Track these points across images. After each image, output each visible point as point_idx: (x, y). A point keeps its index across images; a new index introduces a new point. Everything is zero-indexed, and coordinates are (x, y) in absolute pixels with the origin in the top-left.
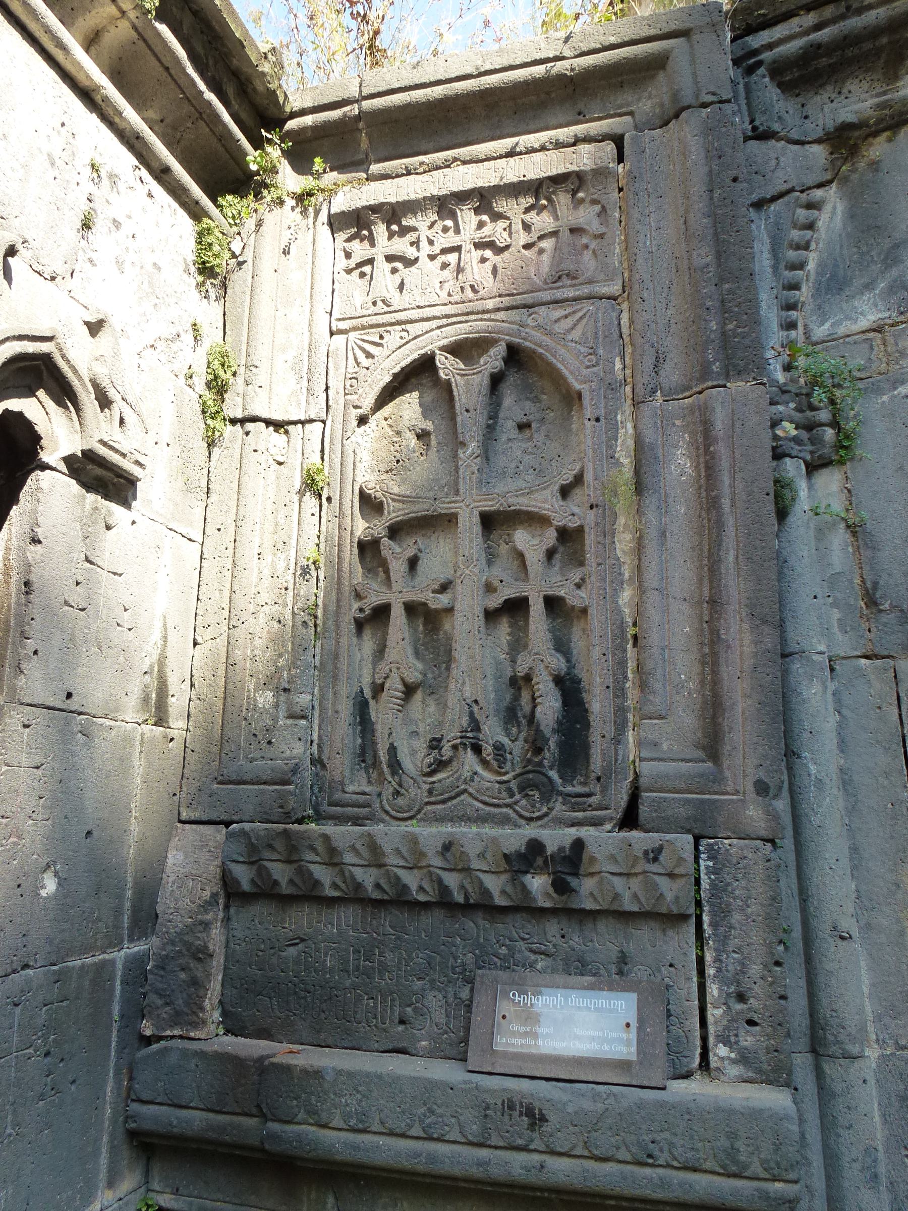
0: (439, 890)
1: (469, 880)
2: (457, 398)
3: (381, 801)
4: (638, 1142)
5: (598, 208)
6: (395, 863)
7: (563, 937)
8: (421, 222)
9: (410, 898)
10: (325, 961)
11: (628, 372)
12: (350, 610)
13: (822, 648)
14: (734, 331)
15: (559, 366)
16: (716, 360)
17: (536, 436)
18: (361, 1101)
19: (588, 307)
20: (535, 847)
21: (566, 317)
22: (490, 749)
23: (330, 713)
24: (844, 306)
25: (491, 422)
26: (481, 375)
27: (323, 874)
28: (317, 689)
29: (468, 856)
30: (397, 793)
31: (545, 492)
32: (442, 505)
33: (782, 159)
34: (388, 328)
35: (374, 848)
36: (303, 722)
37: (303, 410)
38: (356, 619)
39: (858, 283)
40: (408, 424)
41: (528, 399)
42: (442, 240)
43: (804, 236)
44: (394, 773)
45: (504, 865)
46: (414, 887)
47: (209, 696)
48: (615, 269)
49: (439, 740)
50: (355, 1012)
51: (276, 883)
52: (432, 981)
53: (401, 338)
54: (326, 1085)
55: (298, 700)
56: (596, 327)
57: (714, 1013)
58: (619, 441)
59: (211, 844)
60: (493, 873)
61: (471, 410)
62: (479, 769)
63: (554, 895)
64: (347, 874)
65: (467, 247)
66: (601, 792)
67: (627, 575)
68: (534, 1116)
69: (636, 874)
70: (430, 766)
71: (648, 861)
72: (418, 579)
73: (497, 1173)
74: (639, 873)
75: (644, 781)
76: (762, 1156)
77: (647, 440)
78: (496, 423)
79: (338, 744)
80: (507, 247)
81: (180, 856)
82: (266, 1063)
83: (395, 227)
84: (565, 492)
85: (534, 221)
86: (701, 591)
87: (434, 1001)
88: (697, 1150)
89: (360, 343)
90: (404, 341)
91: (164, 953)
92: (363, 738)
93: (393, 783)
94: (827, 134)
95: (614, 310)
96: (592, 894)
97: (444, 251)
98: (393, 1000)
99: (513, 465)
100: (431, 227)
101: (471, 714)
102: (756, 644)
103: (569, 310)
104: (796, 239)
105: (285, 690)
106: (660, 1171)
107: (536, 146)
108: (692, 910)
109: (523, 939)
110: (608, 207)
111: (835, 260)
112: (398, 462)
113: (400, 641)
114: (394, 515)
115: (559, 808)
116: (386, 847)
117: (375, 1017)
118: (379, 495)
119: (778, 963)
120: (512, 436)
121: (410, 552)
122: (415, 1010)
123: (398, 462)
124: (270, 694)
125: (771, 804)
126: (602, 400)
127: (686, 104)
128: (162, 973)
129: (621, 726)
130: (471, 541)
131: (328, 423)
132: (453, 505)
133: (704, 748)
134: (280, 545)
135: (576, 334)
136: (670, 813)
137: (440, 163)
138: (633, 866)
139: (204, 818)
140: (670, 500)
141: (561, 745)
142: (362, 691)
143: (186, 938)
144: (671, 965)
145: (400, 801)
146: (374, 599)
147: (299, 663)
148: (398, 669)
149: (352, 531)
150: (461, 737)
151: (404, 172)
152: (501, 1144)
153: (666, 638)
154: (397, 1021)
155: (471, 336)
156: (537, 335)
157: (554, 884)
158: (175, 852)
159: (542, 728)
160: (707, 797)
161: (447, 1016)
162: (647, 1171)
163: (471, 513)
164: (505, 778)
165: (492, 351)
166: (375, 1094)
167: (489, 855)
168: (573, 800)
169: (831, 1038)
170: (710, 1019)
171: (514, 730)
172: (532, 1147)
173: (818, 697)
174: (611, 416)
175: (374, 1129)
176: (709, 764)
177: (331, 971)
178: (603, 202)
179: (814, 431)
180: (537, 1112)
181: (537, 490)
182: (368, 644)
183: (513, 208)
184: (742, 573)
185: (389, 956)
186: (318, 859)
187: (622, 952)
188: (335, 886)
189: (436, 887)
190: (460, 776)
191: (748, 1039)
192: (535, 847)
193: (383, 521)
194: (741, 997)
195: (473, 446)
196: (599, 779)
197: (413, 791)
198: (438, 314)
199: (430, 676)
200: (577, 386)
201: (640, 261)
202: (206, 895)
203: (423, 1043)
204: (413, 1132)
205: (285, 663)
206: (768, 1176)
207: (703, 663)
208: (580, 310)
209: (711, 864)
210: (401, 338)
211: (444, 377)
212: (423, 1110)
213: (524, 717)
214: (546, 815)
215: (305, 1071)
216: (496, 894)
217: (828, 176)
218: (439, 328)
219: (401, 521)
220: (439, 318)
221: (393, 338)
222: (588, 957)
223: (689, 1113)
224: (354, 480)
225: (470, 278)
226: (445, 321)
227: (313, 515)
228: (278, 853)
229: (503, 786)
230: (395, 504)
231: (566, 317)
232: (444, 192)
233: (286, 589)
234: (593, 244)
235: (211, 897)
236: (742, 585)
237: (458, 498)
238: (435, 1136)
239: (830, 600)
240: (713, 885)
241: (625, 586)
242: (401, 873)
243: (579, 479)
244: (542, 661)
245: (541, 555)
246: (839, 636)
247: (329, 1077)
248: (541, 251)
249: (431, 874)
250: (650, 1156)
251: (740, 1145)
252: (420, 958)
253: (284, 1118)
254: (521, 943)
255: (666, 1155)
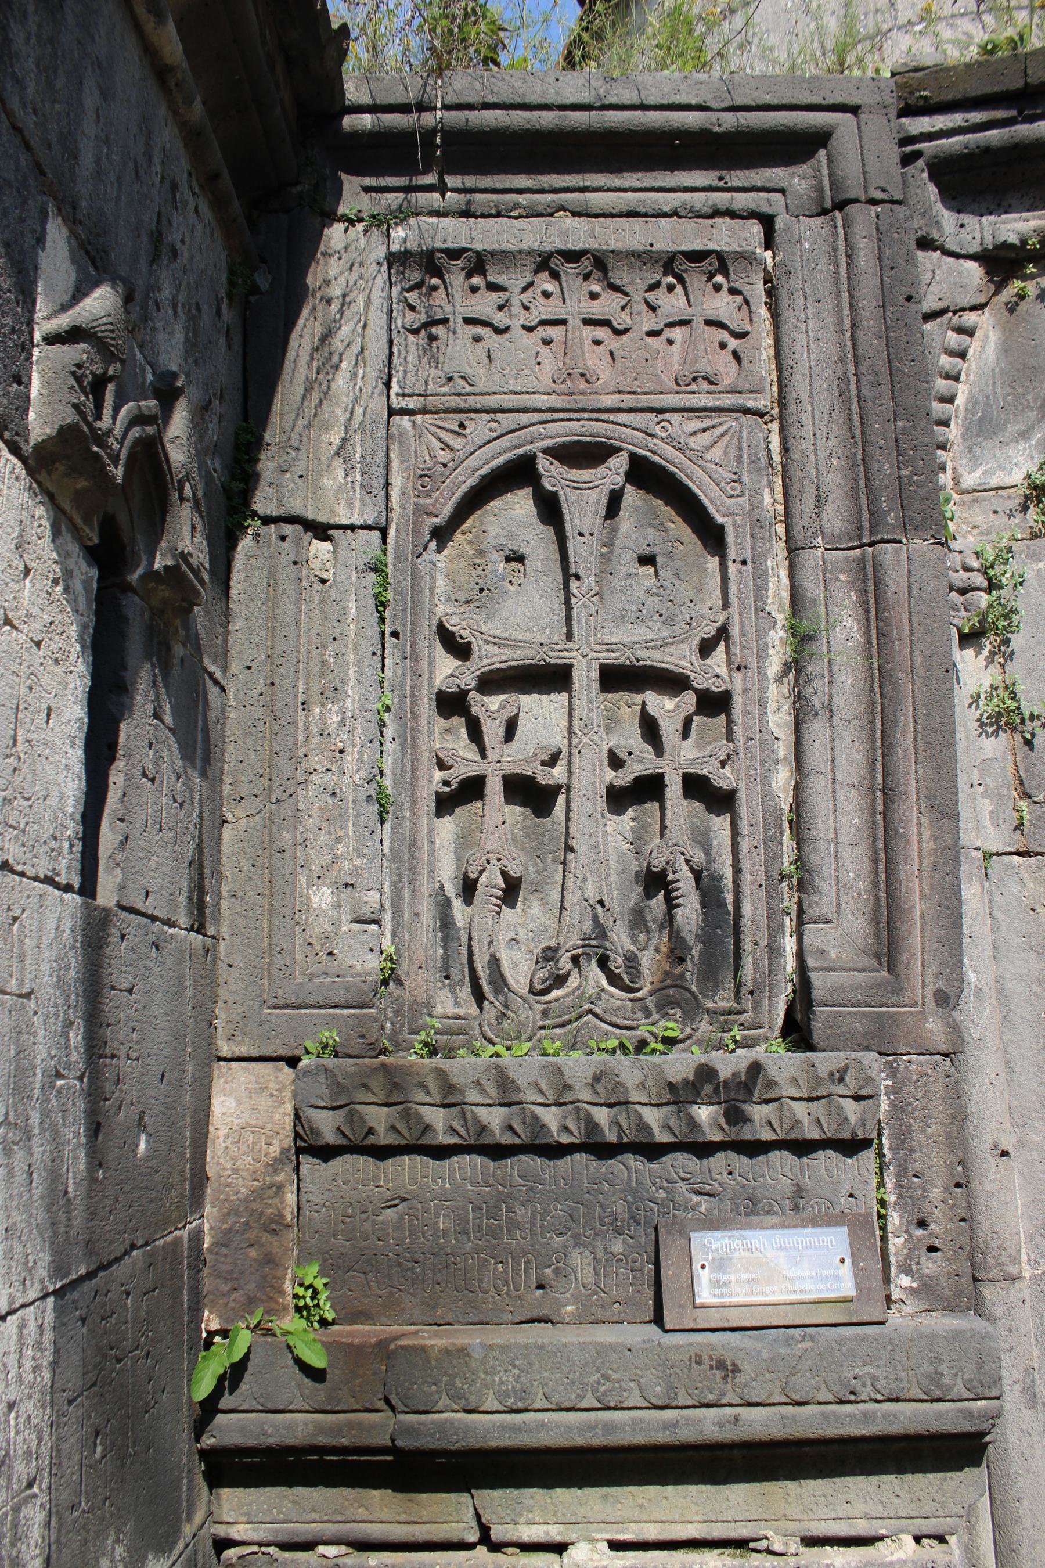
0: (586, 1129)
1: (624, 1115)
2: (567, 517)
3: (480, 1026)
4: (840, 1379)
5: (739, 299)
6: (533, 1099)
7: (730, 1173)
8: (514, 280)
9: (549, 1141)
10: (436, 1223)
11: (781, 508)
12: (430, 782)
13: (979, 844)
14: (909, 478)
15: (697, 491)
16: (891, 510)
17: (661, 573)
18: (519, 1376)
19: (729, 422)
20: (706, 1073)
21: (704, 430)
22: (620, 961)
23: (406, 915)
24: (997, 452)
25: (605, 550)
26: (597, 490)
27: (436, 1118)
28: (387, 884)
29: (624, 1086)
30: (501, 1016)
31: (681, 646)
32: (550, 653)
33: (937, 272)
34: (473, 416)
35: (504, 1082)
36: (374, 927)
37: (357, 511)
38: (437, 793)
39: (1012, 429)
40: (493, 541)
41: (651, 525)
42: (542, 309)
43: (956, 365)
44: (497, 992)
45: (668, 1096)
46: (554, 1126)
47: (249, 893)
48: (762, 379)
49: (555, 950)
50: (480, 1281)
51: (371, 1131)
52: (576, 1236)
53: (491, 430)
54: (473, 1364)
55: (365, 899)
56: (740, 449)
57: (895, 1243)
58: (770, 593)
59: (272, 1085)
60: (652, 1105)
61: (587, 534)
62: (604, 983)
63: (726, 1127)
64: (469, 1116)
65: (574, 322)
66: (754, 1009)
67: (782, 754)
68: (725, 1368)
69: (818, 1098)
70: (544, 981)
71: (833, 1082)
72: (514, 745)
73: (687, 1435)
74: (823, 1097)
75: (817, 994)
76: (966, 1377)
77: (809, 595)
78: (611, 552)
79: (420, 955)
80: (626, 330)
81: (231, 1103)
82: (392, 1347)
83: (476, 280)
84: (706, 648)
85: (659, 303)
86: (873, 777)
87: (580, 1260)
88: (902, 1380)
89: (434, 429)
90: (494, 435)
91: (225, 1226)
92: (445, 947)
93: (497, 1003)
94: (985, 250)
95: (762, 430)
96: (770, 1124)
97: (544, 323)
98: (528, 1262)
99: (634, 608)
100: (525, 289)
101: (595, 918)
102: (935, 840)
103: (707, 423)
104: (947, 367)
105: (346, 885)
106: (861, 1406)
107: (666, 209)
108: (874, 1135)
109: (683, 1180)
110: (751, 300)
111: (987, 397)
112: (481, 590)
113: (500, 824)
114: (486, 661)
115: (704, 1027)
116: (522, 1081)
117: (508, 1285)
118: (464, 633)
119: (958, 1185)
120: (632, 571)
121: (509, 712)
122: (556, 1271)
123: (481, 590)
124: (326, 891)
125: (951, 1016)
126: (749, 539)
127: (853, 197)
128: (224, 1251)
129: (774, 931)
130: (590, 702)
131: (392, 533)
132: (565, 654)
133: (878, 956)
134: (330, 694)
135: (716, 454)
136: (845, 1029)
137: (540, 209)
138: (815, 1089)
139: (255, 1054)
140: (835, 668)
141: (702, 953)
142: (442, 888)
143: (254, 1206)
144: (851, 1196)
145: (506, 1024)
146: (463, 769)
147: (365, 850)
148: (499, 860)
149: (430, 679)
150: (583, 946)
151: (493, 212)
152: (690, 1403)
153: (832, 830)
154: (534, 1285)
155: (583, 439)
156: (668, 451)
157: (726, 1115)
158: (222, 1098)
159: (683, 934)
160: (885, 1009)
161: (596, 1274)
162: (849, 1408)
163: (589, 666)
164: (638, 995)
165: (612, 462)
166: (536, 1366)
167: (650, 1083)
168: (722, 1018)
169: (991, 1261)
170: (892, 1250)
171: (642, 937)
172: (723, 1402)
173: (978, 898)
174: (758, 560)
175: (536, 1406)
176: (885, 974)
177: (446, 1234)
178: (745, 293)
179: (968, 595)
180: (729, 1363)
181: (672, 644)
182: (447, 828)
183: (635, 281)
184: (920, 759)
185: (520, 1210)
186: (428, 1099)
187: (797, 1185)
188: (453, 1131)
189: (583, 1126)
190: (583, 993)
191: (930, 1265)
192: (706, 1073)
193: (472, 669)
194: (922, 1224)
195: (589, 581)
196: (751, 993)
197: (524, 1014)
198: (539, 405)
199: (531, 869)
200: (720, 519)
201: (797, 377)
202: (275, 1150)
203: (569, 1308)
204: (585, 1404)
205: (345, 850)
206: (971, 1396)
207: (875, 861)
208: (721, 424)
209: (890, 1083)
210: (491, 430)
211: (548, 487)
212: (596, 1377)
213: (654, 921)
214: (689, 1037)
215: (446, 1352)
216: (656, 1129)
217: (982, 300)
218: (541, 423)
219: (498, 669)
220: (540, 411)
221: (479, 428)
222: (759, 1193)
223: (891, 1344)
224: (431, 612)
225: (581, 364)
226: (548, 416)
227: (374, 654)
228: (374, 1094)
229: (638, 1004)
230: (488, 647)
231: (704, 430)
232: (548, 248)
233: (341, 752)
234: (733, 343)
235: (281, 1153)
236: (920, 773)
237: (571, 645)
238: (612, 1404)
239: (982, 789)
240: (893, 1105)
241: (780, 766)
242: (539, 1111)
243: (723, 633)
244: (682, 854)
245: (679, 726)
246: (990, 828)
247: (477, 1354)
248: (670, 342)
249: (578, 1109)
250: (852, 1393)
251: (944, 1369)
252: (559, 1211)
253: (422, 1408)
254: (681, 1184)
255: (869, 1389)
